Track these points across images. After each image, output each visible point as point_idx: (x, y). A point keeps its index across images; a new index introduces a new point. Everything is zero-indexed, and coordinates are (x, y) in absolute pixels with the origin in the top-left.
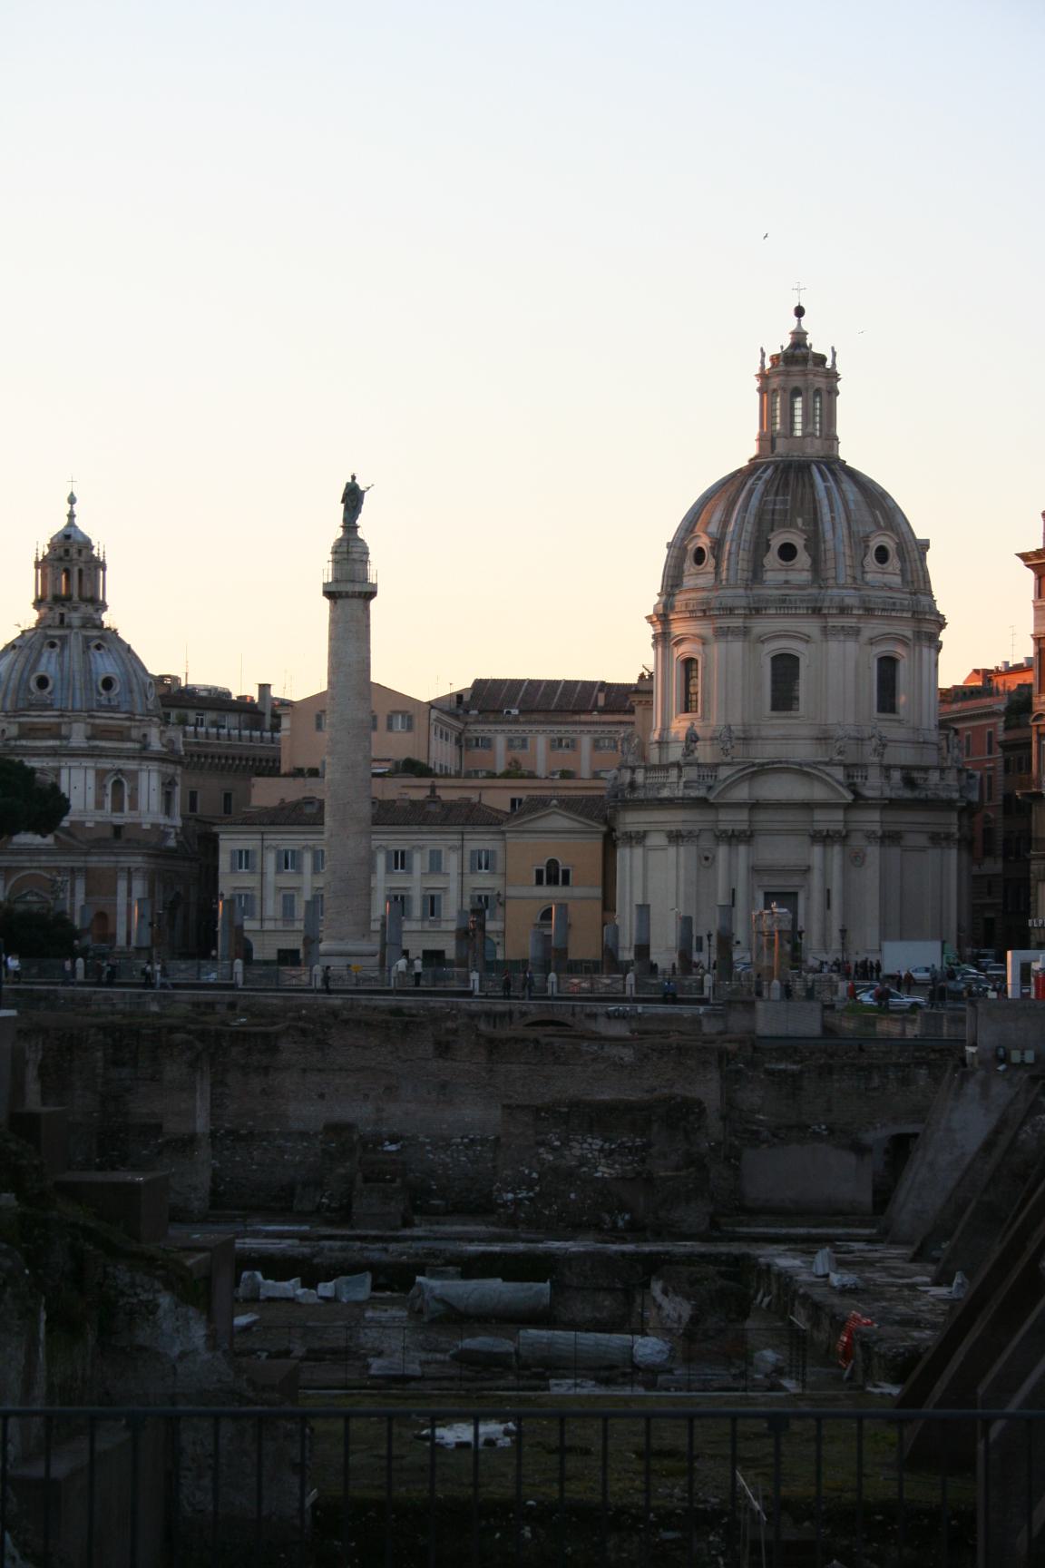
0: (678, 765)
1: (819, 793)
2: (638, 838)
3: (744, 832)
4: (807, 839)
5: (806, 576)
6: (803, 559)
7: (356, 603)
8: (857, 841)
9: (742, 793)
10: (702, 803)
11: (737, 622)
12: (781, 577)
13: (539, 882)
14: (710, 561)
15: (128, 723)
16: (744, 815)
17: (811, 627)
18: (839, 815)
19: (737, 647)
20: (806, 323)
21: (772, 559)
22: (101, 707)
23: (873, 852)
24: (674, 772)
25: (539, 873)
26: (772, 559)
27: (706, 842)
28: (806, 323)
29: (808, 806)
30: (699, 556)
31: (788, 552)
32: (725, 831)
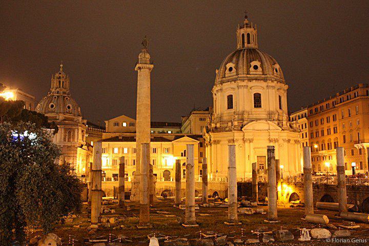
2: (217, 142)
5: (261, 73)
6: (260, 69)
8: (281, 141)
12: (255, 73)
13: (182, 156)
14: (234, 70)
15: (74, 117)
17: (264, 84)
19: (245, 90)
21: (252, 69)
22: (67, 113)
23: (286, 144)
25: (182, 153)
26: (252, 69)
31: (256, 67)
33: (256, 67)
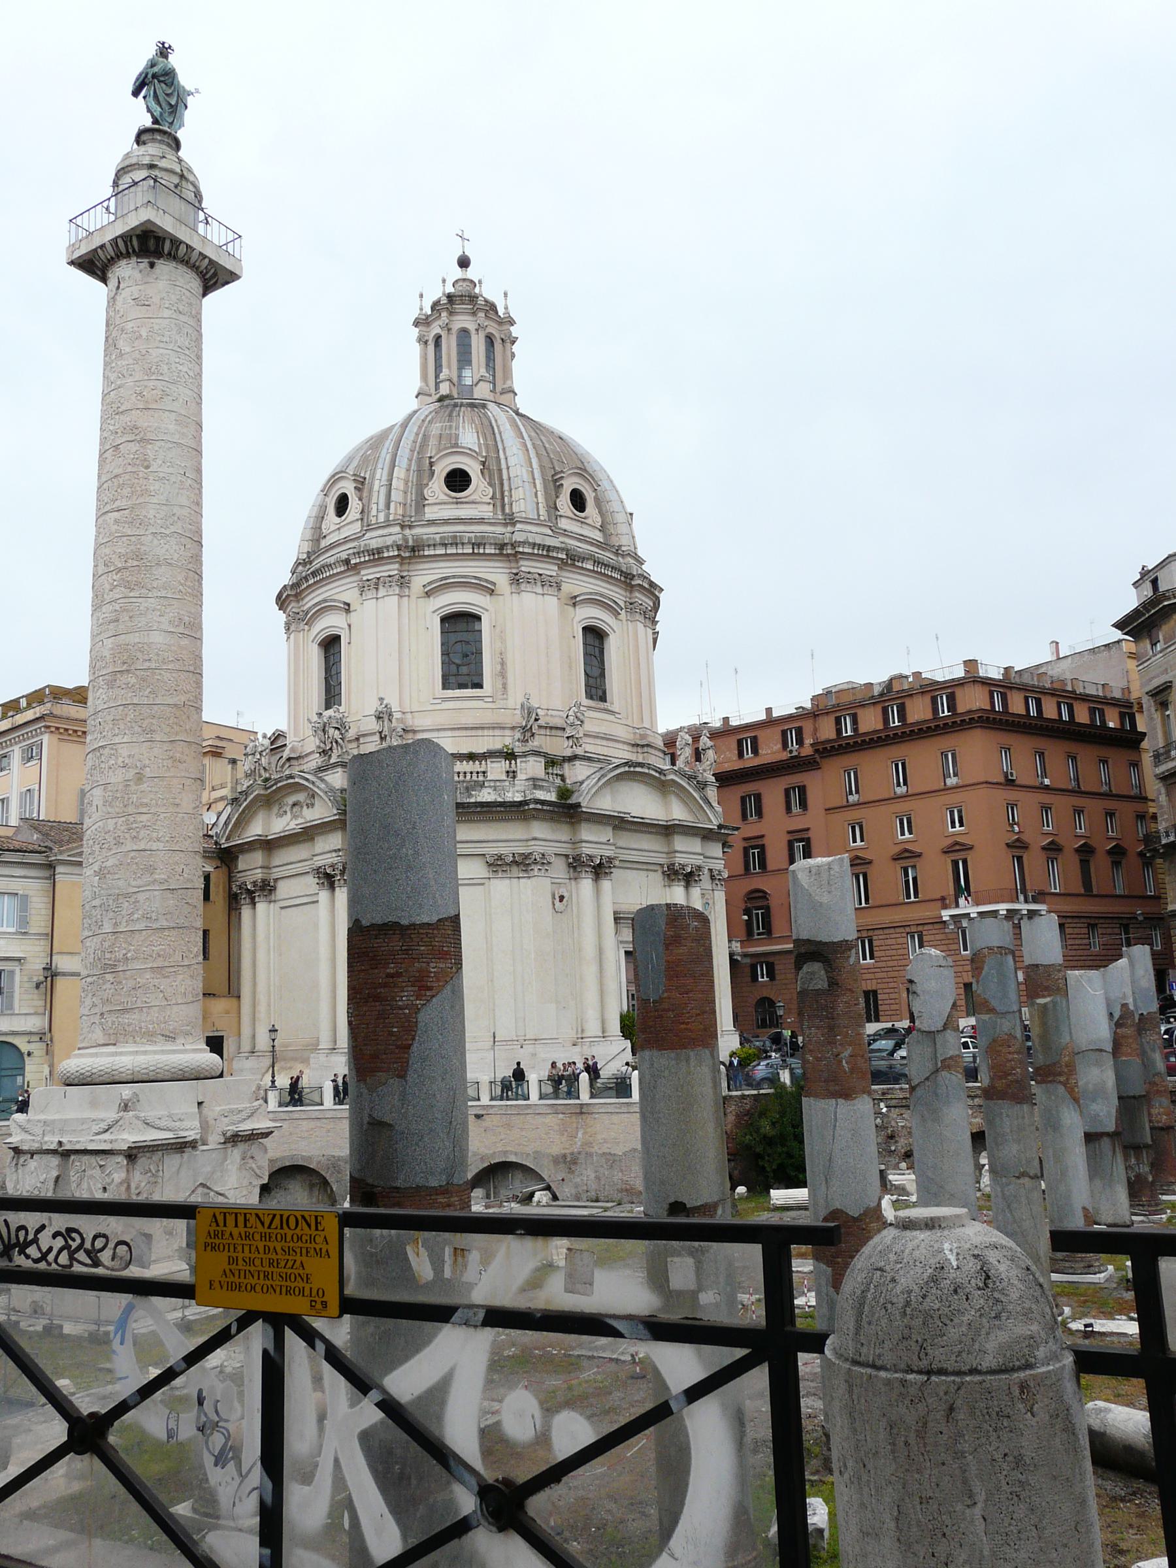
0: (510, 756)
1: (678, 812)
3: (610, 860)
4: (657, 877)
7: (190, 281)
9: (606, 804)
10: (566, 810)
11: (550, 569)
16: (604, 834)
18: (695, 845)
20: (471, 273)
21: (564, 503)
24: (496, 769)
27: (559, 869)
28: (471, 273)
29: (668, 830)
30: (458, 480)
32: (591, 857)
33: (578, 500)
